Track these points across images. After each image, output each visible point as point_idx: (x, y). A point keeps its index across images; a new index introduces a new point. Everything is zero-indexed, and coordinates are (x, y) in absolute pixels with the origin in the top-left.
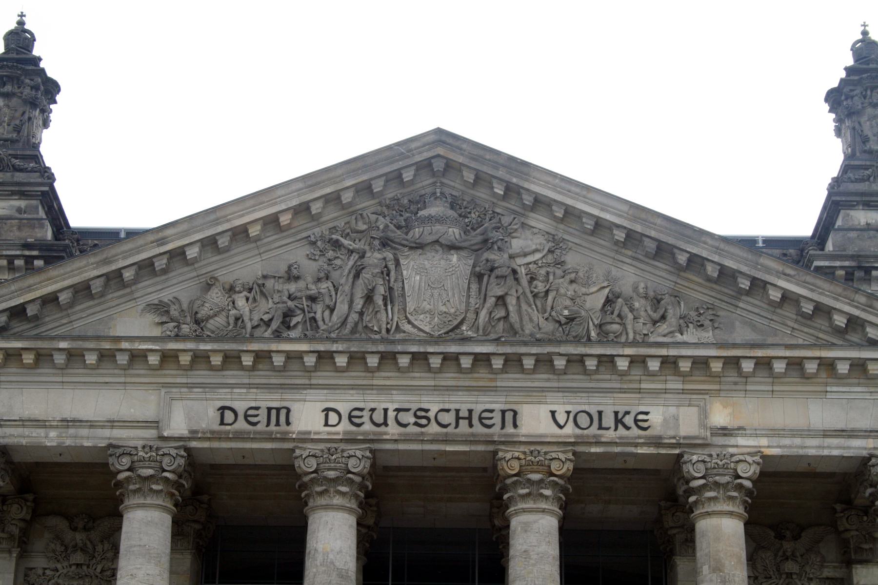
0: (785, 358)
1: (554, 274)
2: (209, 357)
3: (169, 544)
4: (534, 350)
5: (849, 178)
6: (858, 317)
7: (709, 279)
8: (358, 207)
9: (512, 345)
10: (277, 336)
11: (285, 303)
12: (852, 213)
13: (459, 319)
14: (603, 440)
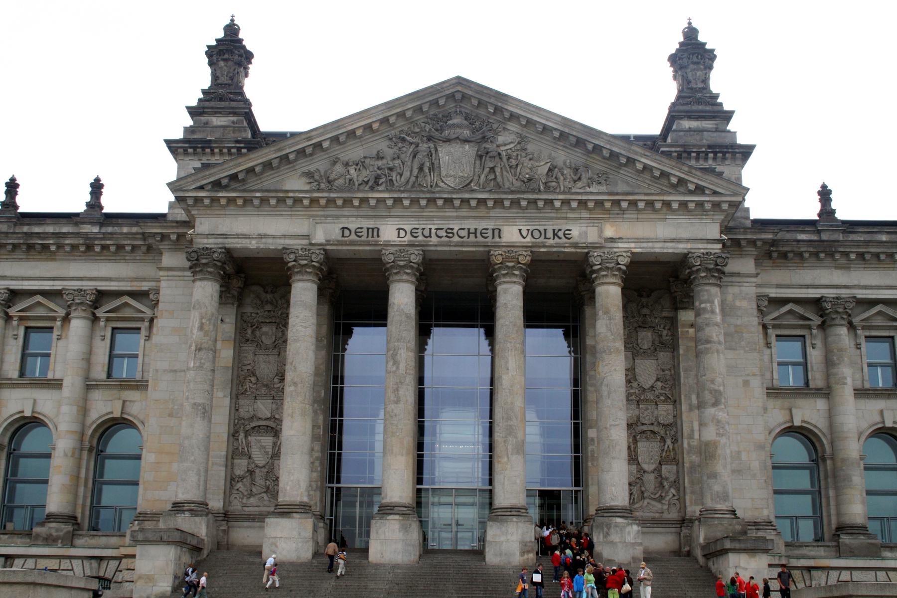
1: (521, 155)
2: (335, 201)
3: (316, 300)
4: (510, 196)
5: (680, 103)
6: (683, 178)
7: (604, 158)
8: (415, 119)
10: (372, 189)
12: (681, 122)
13: (470, 180)
14: (547, 244)
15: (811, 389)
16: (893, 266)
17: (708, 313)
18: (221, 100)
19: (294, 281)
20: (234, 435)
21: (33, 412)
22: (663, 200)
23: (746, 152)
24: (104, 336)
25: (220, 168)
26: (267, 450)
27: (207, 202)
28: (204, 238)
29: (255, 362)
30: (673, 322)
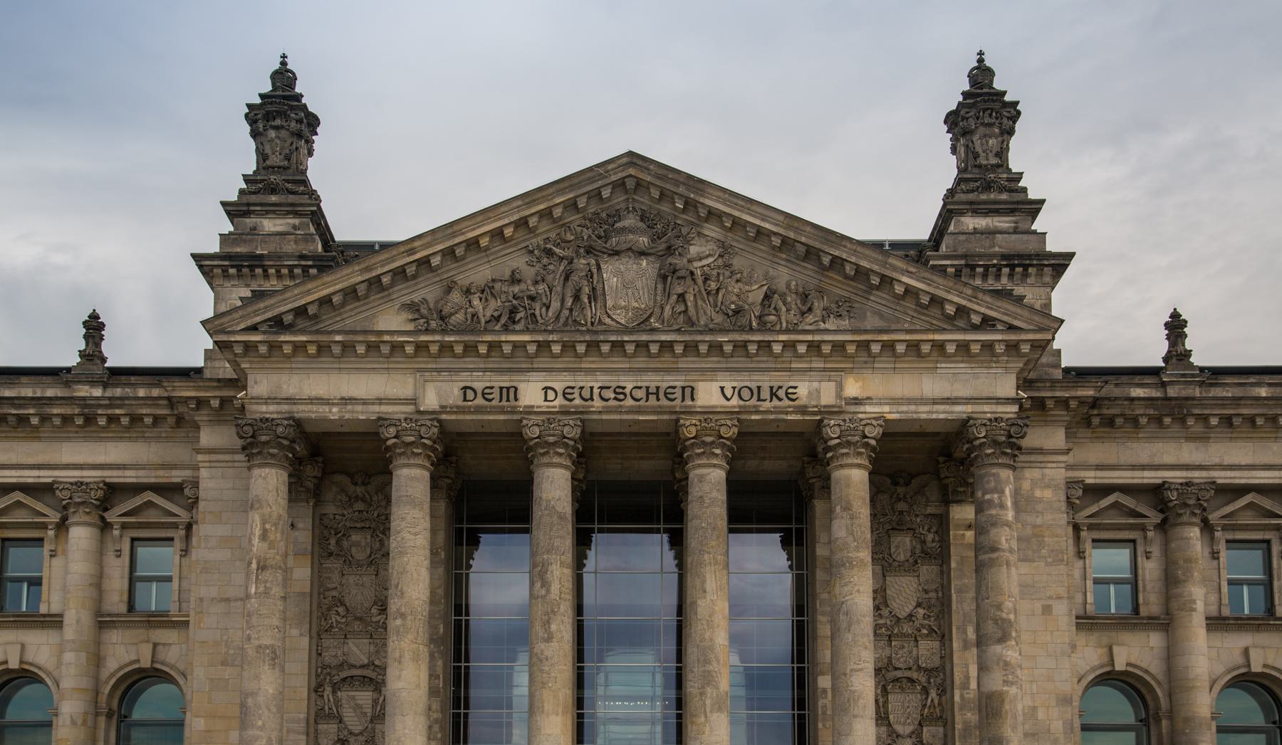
0: (906, 341)
4: (708, 338)
9: (691, 334)
10: (506, 329)
11: (511, 302)
12: (963, 219)
13: (648, 313)
14: (761, 409)
15: (1143, 618)
16: (1274, 435)
17: (995, 508)
18: (273, 191)
19: (395, 467)
20: (317, 689)
21: (21, 662)
23: (1060, 263)
24: (120, 551)
25: (280, 298)
26: (365, 710)
27: (263, 349)
28: (261, 404)
29: (343, 586)
30: (942, 523)
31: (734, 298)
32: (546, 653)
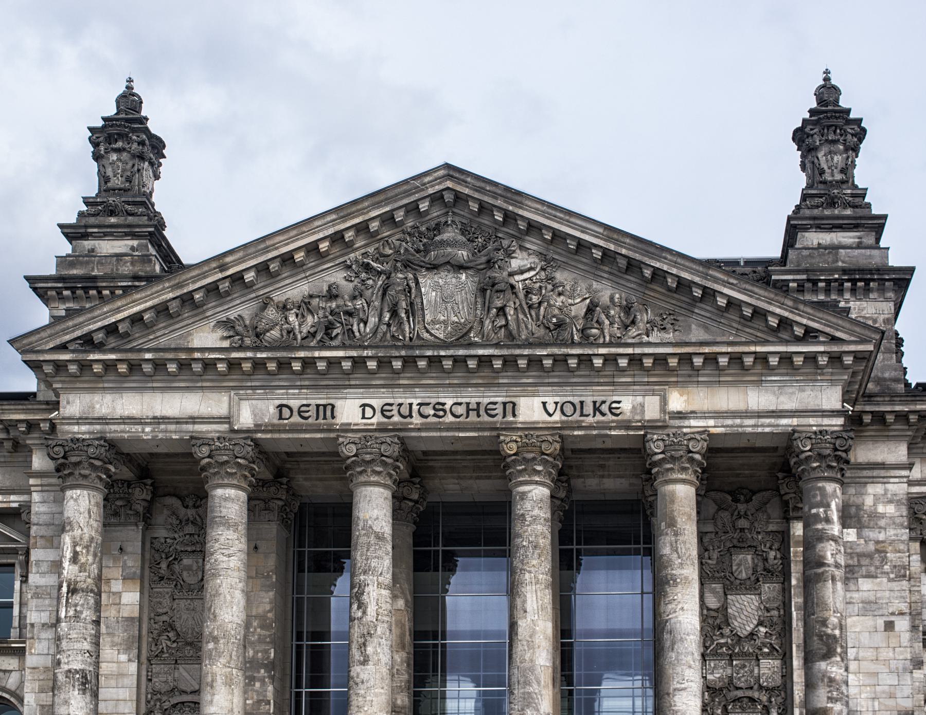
0: (728, 353)
1: (546, 288)
3: (245, 516)
4: (526, 352)
5: (807, 205)
9: (508, 348)
11: (327, 317)
12: (807, 234)
13: (468, 327)
14: (584, 424)
18: (112, 213)
22: (755, 353)
31: (556, 312)
32: (362, 676)
